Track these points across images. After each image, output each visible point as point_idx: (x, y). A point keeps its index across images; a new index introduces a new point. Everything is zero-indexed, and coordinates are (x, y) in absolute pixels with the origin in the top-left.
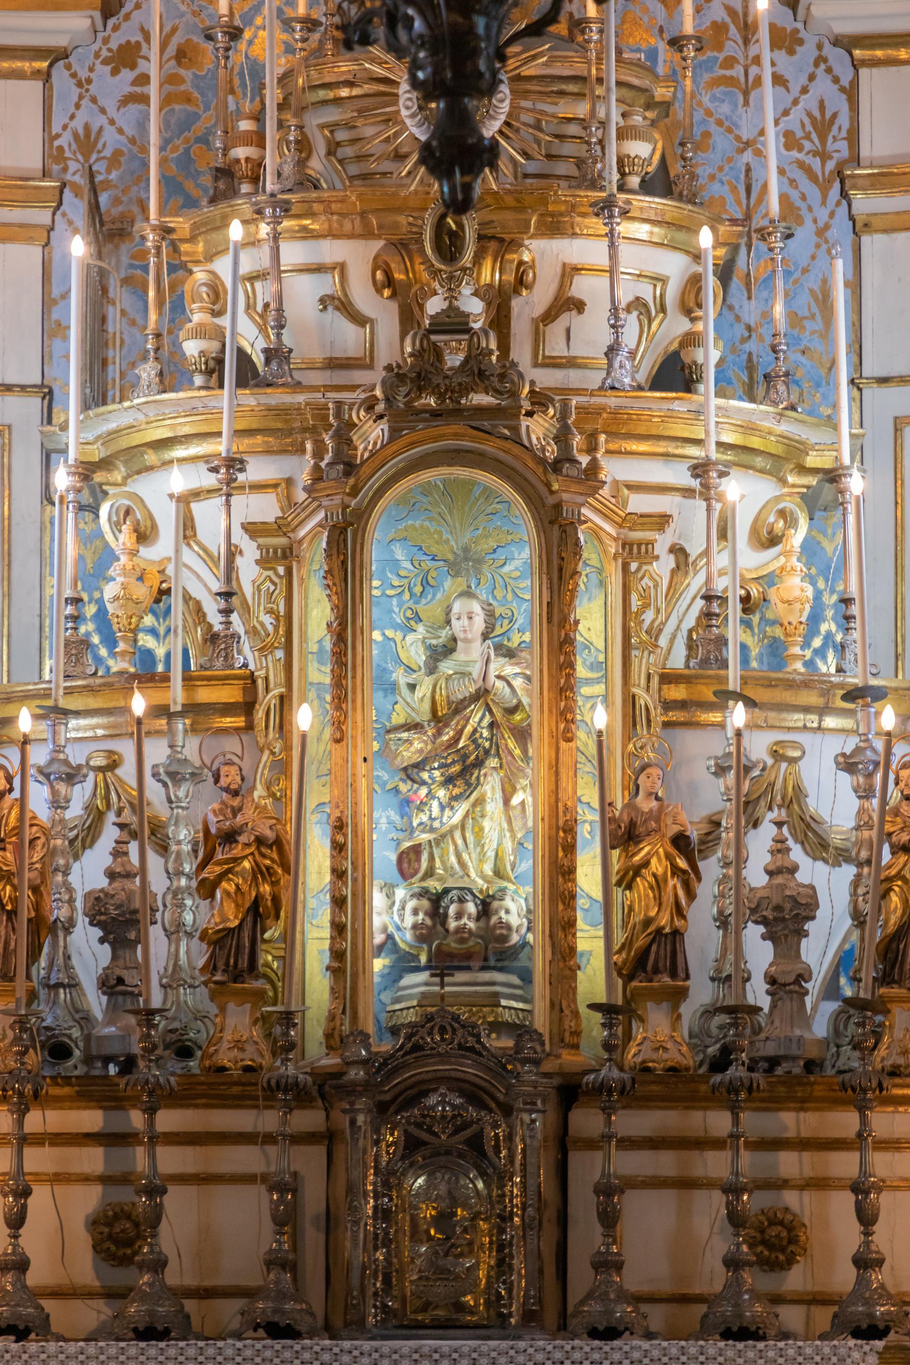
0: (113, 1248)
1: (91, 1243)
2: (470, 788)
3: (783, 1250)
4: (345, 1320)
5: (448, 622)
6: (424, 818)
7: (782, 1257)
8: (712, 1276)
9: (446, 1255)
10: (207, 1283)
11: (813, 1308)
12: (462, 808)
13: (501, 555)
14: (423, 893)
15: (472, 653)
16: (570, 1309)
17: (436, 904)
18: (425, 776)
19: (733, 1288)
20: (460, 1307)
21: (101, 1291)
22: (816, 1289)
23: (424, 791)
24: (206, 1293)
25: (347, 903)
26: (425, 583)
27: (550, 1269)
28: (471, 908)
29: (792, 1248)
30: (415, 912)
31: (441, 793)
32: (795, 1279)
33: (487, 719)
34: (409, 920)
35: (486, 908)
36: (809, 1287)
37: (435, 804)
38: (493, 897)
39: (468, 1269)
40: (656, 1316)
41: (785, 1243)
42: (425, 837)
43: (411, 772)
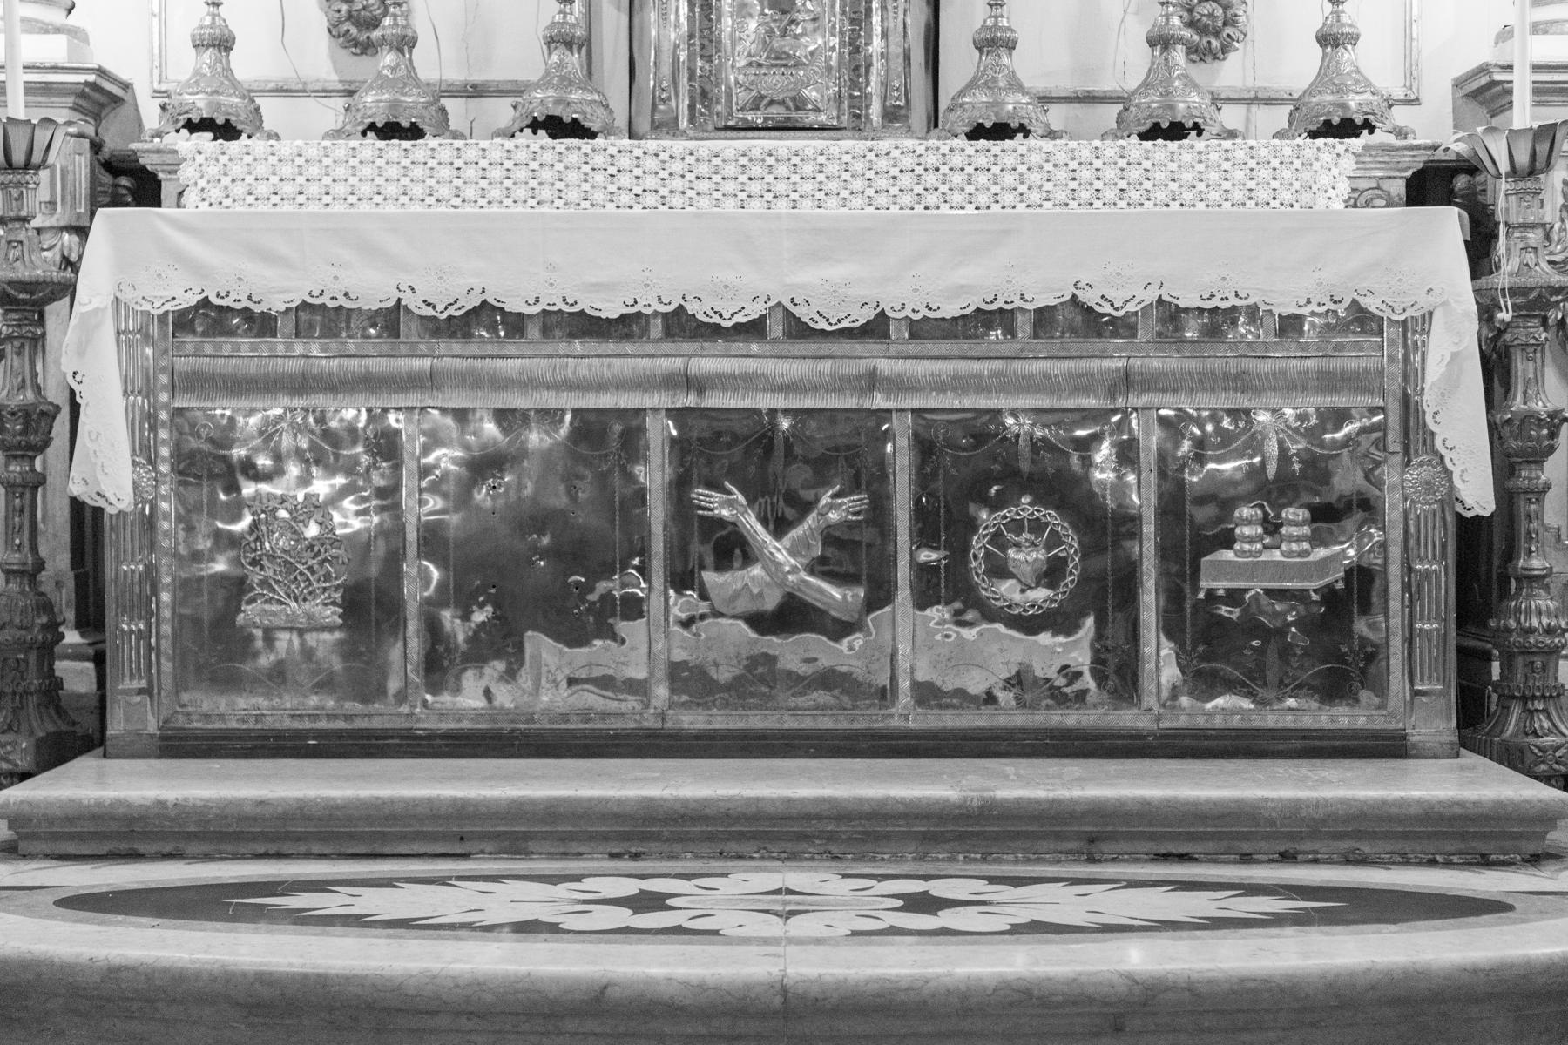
0: (354, 31)
1: (326, 24)
3: (1217, 34)
4: (653, 121)
7: (1215, 43)
8: (1126, 65)
9: (783, 35)
10: (477, 77)
11: (1254, 108)
16: (942, 107)
19: (1156, 79)
20: (800, 104)
21: (340, 87)
22: (1258, 84)
24: (475, 91)
27: (918, 56)
29: (1229, 30)
32: (1231, 73)
36: (1249, 84)
39: (812, 53)
40: (1057, 116)
41: (1220, 24)
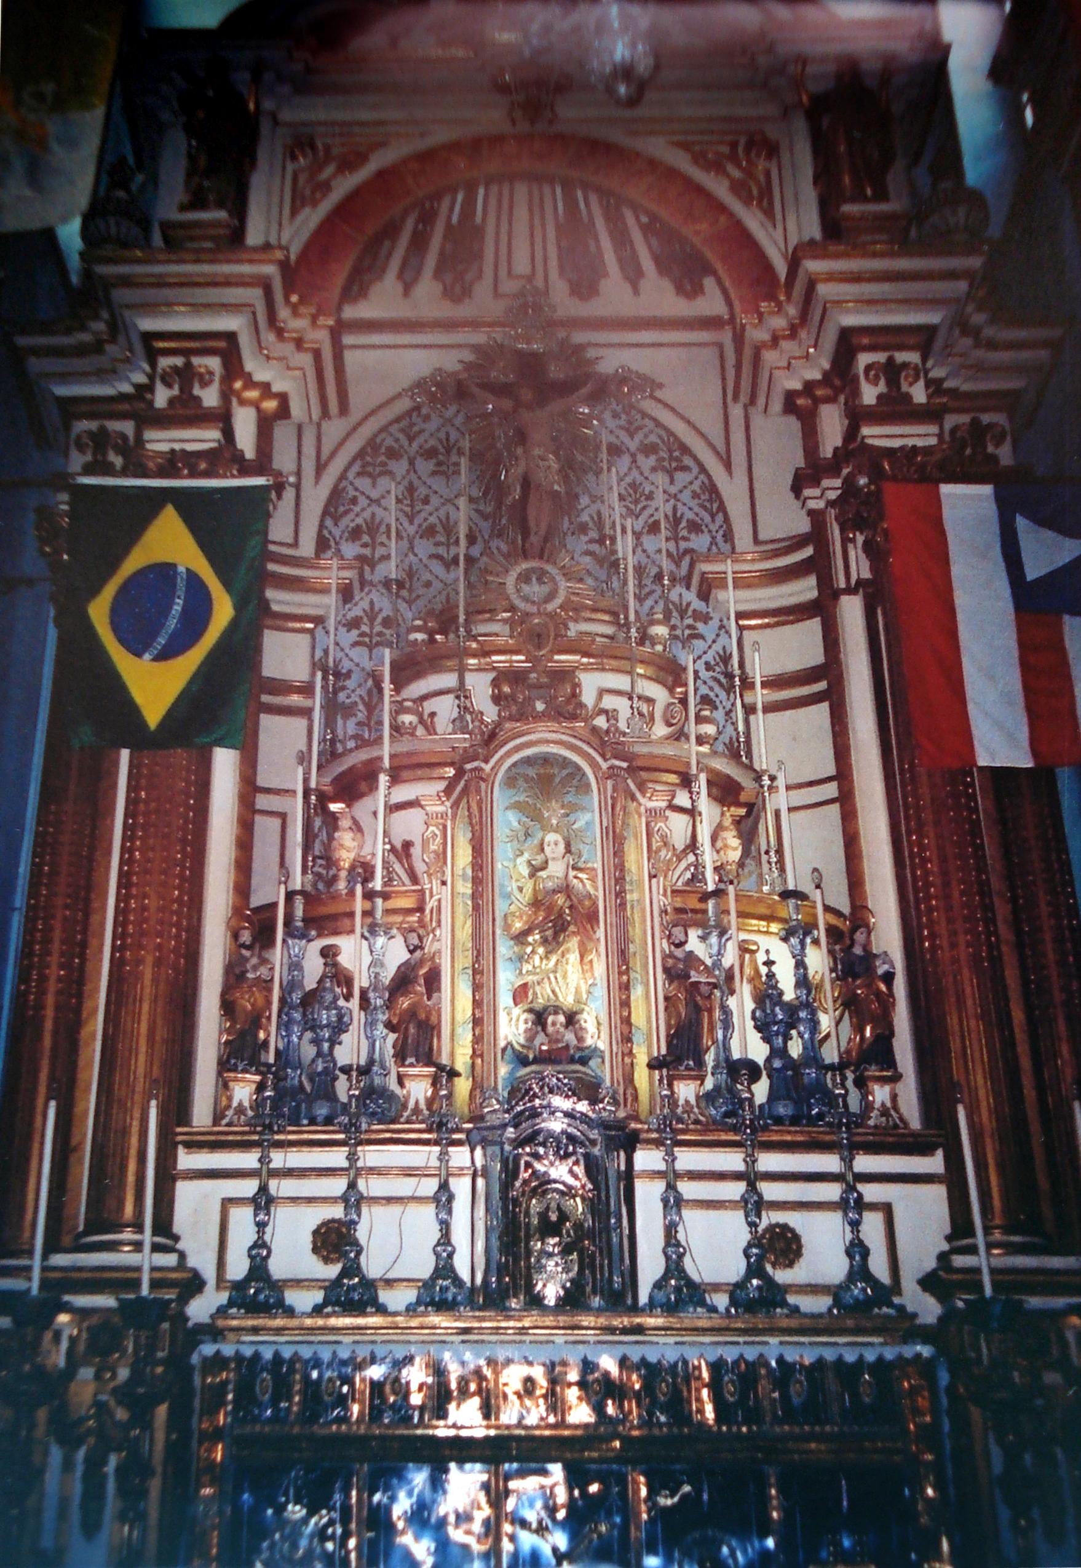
2: (559, 944)
5: (543, 850)
6: (530, 968)
12: (554, 959)
13: (572, 818)
14: (530, 1011)
15: (556, 870)
17: (540, 1018)
18: (530, 939)
23: (529, 950)
25: (482, 1019)
26: (527, 835)
28: (561, 1018)
30: (526, 1022)
31: (541, 950)
33: (568, 904)
34: (522, 1027)
35: (571, 1019)
37: (537, 958)
38: (576, 1013)
42: (529, 979)
43: (520, 938)
